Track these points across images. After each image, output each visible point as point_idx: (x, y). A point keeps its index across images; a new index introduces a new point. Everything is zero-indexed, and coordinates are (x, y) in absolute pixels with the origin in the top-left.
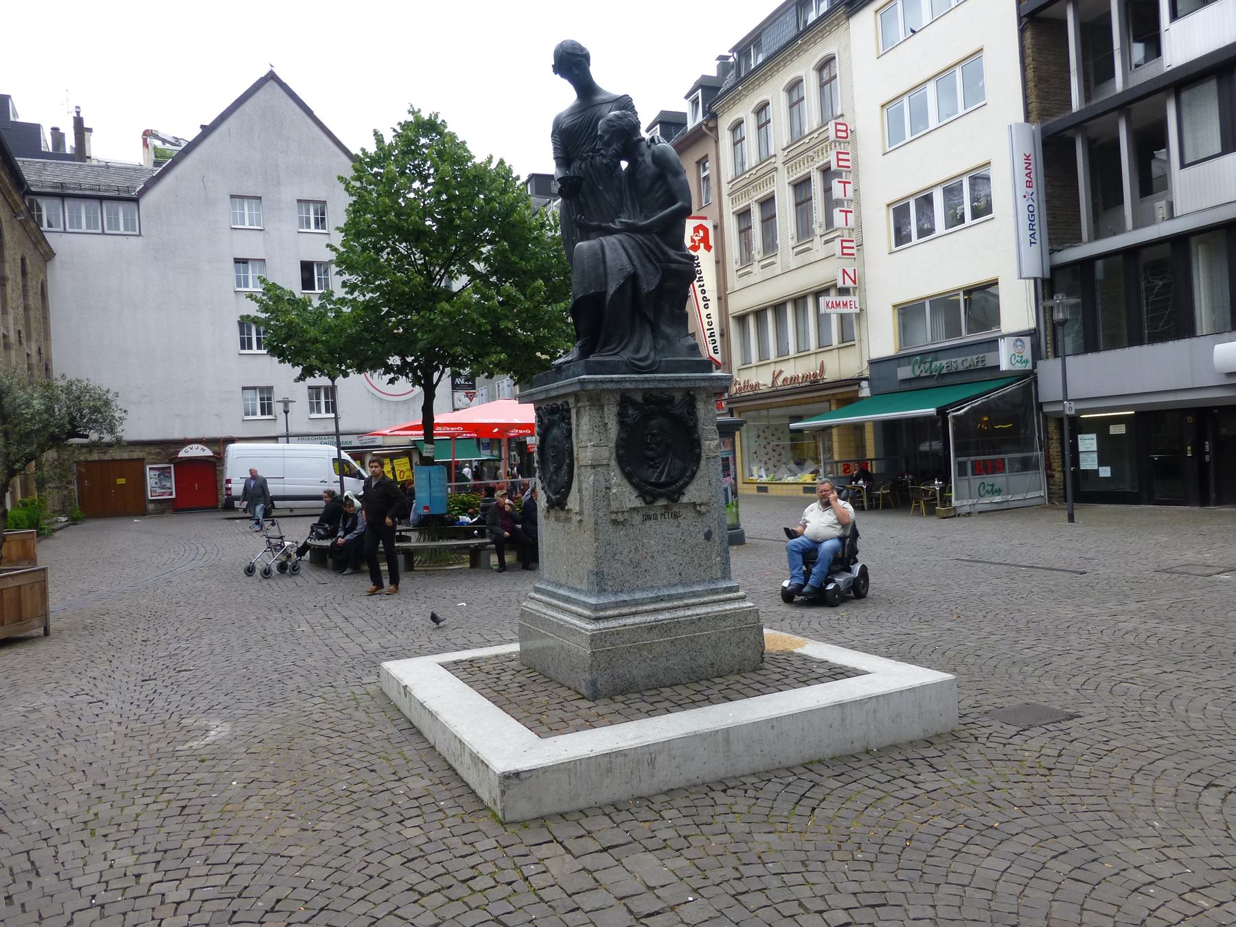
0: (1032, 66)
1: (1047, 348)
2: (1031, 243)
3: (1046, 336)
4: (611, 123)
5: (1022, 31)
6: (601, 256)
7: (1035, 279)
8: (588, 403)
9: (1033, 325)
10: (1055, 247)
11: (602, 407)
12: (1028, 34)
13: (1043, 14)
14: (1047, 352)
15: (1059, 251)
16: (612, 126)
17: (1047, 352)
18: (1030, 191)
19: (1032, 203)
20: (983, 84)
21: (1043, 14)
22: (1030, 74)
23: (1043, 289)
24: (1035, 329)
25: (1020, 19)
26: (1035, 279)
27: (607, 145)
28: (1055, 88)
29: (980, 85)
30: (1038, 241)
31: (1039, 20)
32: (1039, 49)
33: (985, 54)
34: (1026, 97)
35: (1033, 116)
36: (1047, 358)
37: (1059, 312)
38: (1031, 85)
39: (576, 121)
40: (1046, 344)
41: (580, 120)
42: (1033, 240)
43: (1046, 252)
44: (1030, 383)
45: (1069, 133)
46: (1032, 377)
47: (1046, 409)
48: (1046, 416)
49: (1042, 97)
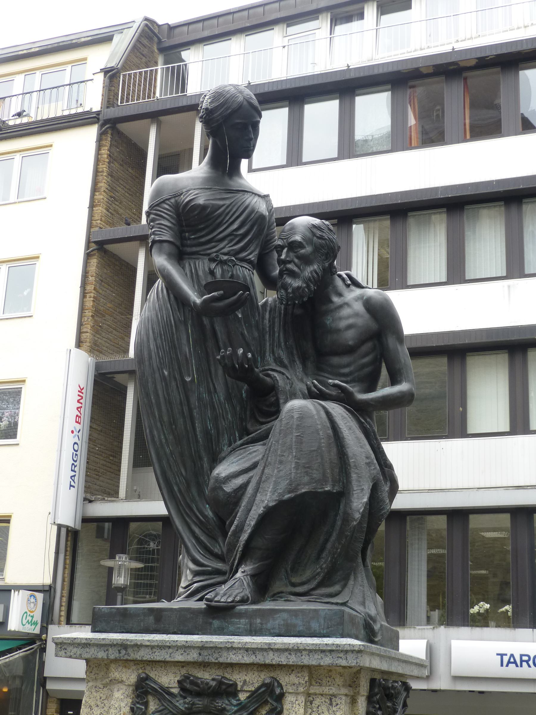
0: (92, 295)
1: (60, 611)
2: (71, 486)
3: (62, 596)
4: (319, 233)
5: (88, 256)
6: (330, 432)
7: (60, 527)
8: (344, 691)
9: (48, 580)
10: (89, 496)
11: (353, 701)
12: (94, 261)
13: (109, 247)
14: (60, 616)
15: (90, 501)
16: (321, 238)
17: (60, 616)
18: (78, 427)
19: (77, 441)
20: (30, 294)
21: (109, 247)
22: (89, 303)
23: (67, 540)
24: (50, 586)
25: (88, 242)
26: (60, 527)
27: (306, 260)
28: (108, 325)
29: (25, 293)
30: (76, 485)
31: (106, 252)
32: (101, 280)
33: (39, 264)
34: (80, 324)
35: (86, 345)
36: (59, 623)
37: (119, 575)
38: (88, 314)
39: (221, 203)
40: (61, 606)
41: (228, 202)
42: (72, 483)
43: (81, 499)
44: (35, 652)
45: (119, 378)
46: (38, 643)
47: (50, 686)
48: (47, 694)
49: (97, 330)
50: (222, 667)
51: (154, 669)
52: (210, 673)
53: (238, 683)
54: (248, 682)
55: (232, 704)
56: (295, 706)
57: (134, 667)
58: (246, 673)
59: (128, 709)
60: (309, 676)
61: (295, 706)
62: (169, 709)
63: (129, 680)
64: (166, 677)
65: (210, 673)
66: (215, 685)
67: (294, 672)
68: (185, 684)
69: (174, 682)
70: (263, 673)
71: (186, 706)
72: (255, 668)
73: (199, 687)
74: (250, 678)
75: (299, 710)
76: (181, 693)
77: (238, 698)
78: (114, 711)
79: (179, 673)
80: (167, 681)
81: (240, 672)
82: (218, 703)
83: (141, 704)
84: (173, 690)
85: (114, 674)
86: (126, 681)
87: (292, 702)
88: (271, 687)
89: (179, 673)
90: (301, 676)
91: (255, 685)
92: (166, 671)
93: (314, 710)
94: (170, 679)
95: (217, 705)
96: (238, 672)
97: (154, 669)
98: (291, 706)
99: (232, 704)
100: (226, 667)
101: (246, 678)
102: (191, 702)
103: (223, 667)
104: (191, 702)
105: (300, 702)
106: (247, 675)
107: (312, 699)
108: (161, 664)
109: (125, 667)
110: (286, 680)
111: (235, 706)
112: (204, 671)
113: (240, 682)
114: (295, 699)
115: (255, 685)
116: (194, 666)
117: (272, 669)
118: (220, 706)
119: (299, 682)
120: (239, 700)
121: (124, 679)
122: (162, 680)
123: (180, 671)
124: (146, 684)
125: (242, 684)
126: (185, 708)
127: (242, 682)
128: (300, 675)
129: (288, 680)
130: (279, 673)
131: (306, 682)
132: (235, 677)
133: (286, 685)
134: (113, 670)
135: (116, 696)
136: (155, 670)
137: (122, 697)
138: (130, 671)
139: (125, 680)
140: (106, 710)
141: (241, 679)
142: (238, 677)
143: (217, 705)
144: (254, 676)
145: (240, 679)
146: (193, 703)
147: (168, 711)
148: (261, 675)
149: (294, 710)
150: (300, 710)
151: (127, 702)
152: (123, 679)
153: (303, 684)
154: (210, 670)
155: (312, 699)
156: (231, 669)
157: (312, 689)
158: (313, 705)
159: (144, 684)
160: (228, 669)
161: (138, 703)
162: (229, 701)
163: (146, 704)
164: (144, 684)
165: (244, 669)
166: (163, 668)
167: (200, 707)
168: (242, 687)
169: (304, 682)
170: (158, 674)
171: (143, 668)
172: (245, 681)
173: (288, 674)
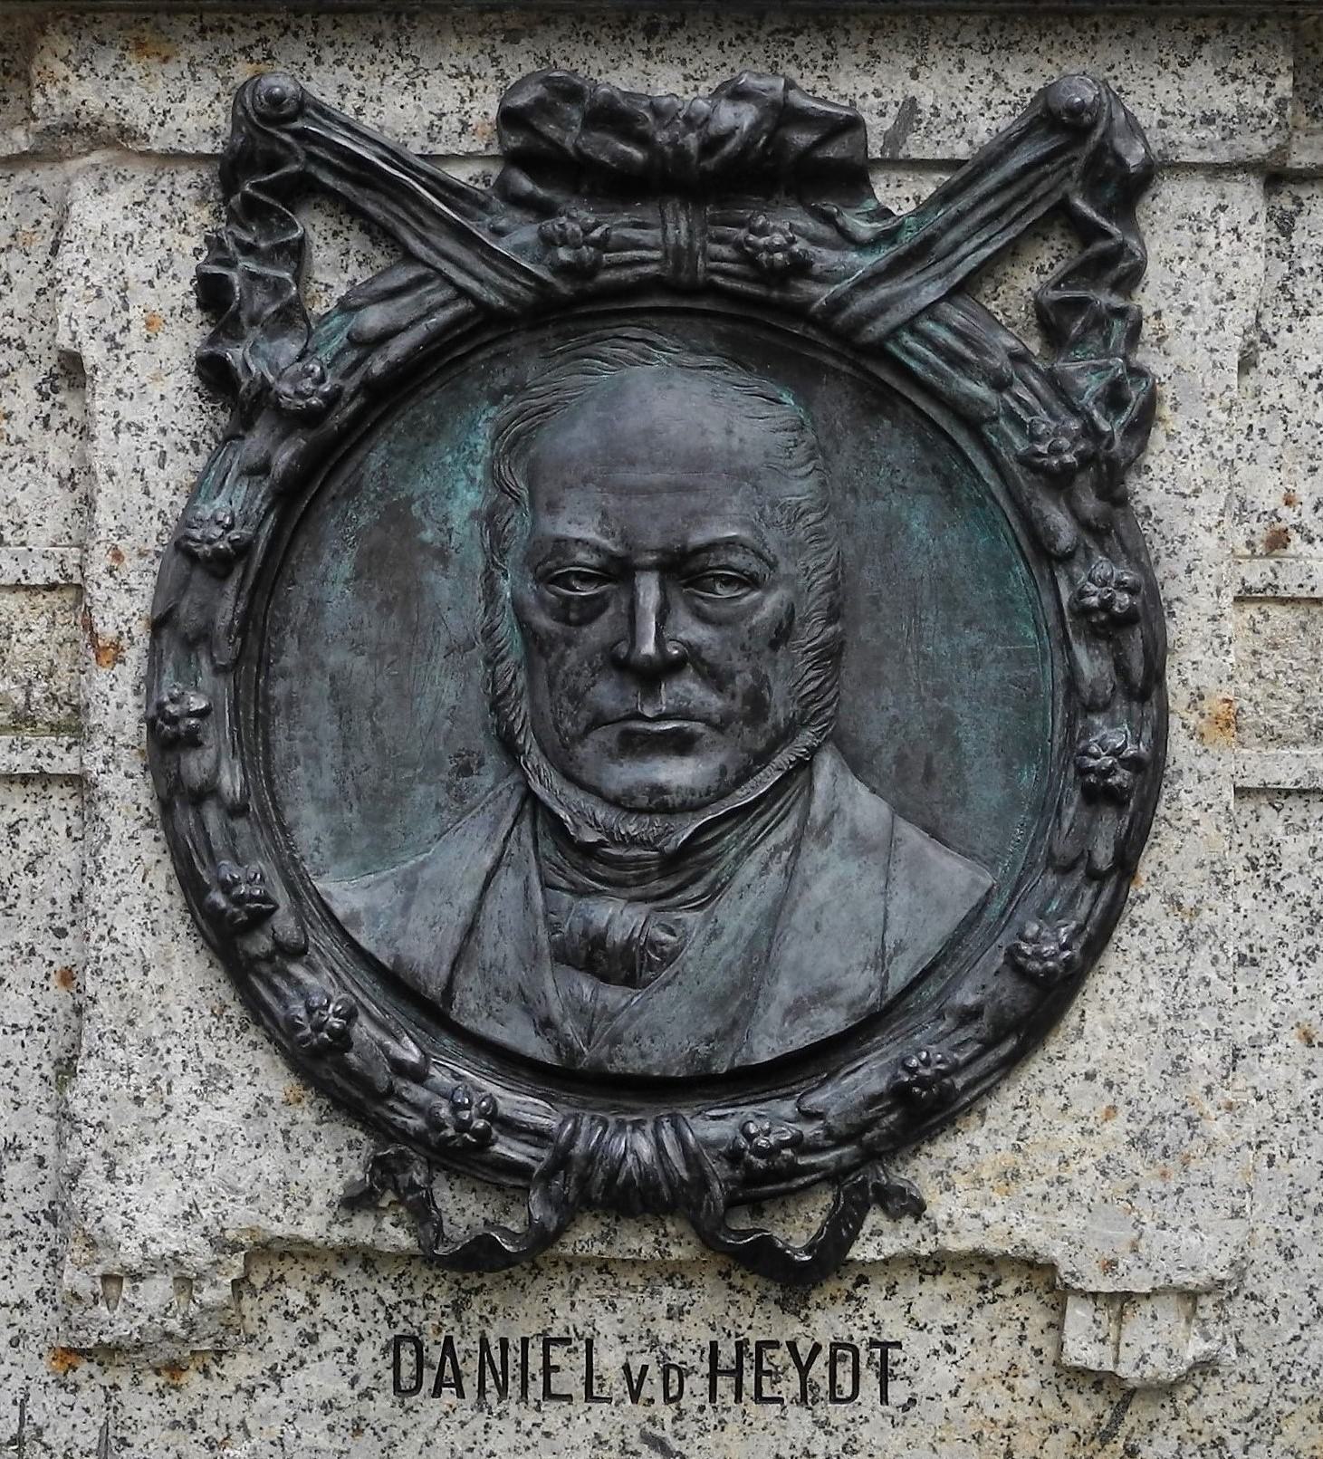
50: (763, 37)
51: (328, 55)
52: (690, 70)
53: (870, 119)
54: (928, 111)
55: (848, 240)
56: (1210, 239)
57: (198, 50)
58: (911, 64)
59: (180, 290)
60: (1295, 69)
61: (1210, 239)
62: (449, 281)
63: (170, 125)
64: (407, 98)
65: (690, 70)
66: (755, 126)
67: (1206, 50)
68: (551, 129)
69: (465, 125)
70: (1021, 61)
71: (564, 255)
72: (969, 35)
73: (643, 141)
74: (942, 89)
75: (1236, 264)
76: (525, 184)
77: (870, 205)
78: (82, 311)
79: (492, 72)
80: (421, 122)
81: (875, 56)
82: (762, 231)
83: (266, 258)
84: (460, 174)
85: (65, 92)
86: (153, 132)
87: (1196, 217)
88: (1099, 131)
89: (492, 72)
90: (1254, 69)
91: (969, 126)
92: (406, 66)
93: (1305, 264)
94: (436, 108)
95: (762, 241)
96: (862, 57)
97: (328, 55)
98: (1187, 243)
99: (848, 240)
100: (787, 30)
101: (915, 89)
102: (596, 234)
103: (768, 28)
104: (596, 234)
105: (1244, 219)
106: (921, 70)
107: (1289, 207)
108: (375, 27)
109: (140, 46)
110: (1161, 97)
111: (862, 246)
112: (648, 54)
113: (881, 114)
114: (1212, 201)
115: (969, 126)
116: (586, 27)
117: (1073, 35)
118: (779, 248)
119: (1240, 107)
120: (885, 213)
121: (139, 117)
122: (386, 119)
123: (496, 61)
124: (301, 135)
125: (888, 123)
126: (562, 270)
127: (893, 111)
128: (1244, 65)
129: (1175, 96)
130: (1116, 54)
131: (1281, 103)
132: (844, 87)
133: (1162, 125)
134: (61, 69)
135: (94, 222)
136: (339, 62)
137: (132, 225)
138: (172, 70)
139: (142, 124)
140: (22, 311)
141: (887, 97)
142: (866, 84)
143: (762, 241)
144: (963, 79)
145: (877, 94)
146: (605, 237)
147: (449, 292)
148: (1008, 74)
149: (1208, 261)
150: (1244, 261)
151: (162, 253)
152: (128, 120)
153: (1263, 116)
154: (688, 52)
155: (1289, 207)
156: (822, 41)
157: (1304, 148)
158: (1298, 238)
159: (287, 138)
160: (800, 42)
161: (248, 250)
162: (828, 219)
163: (297, 253)
164: (287, 138)
165: (902, 42)
166: (391, 45)
167: (643, 262)
168: (892, 139)
169: (1270, 102)
170: (360, 83)
171: (258, 53)
172: (910, 108)
173: (1174, 66)
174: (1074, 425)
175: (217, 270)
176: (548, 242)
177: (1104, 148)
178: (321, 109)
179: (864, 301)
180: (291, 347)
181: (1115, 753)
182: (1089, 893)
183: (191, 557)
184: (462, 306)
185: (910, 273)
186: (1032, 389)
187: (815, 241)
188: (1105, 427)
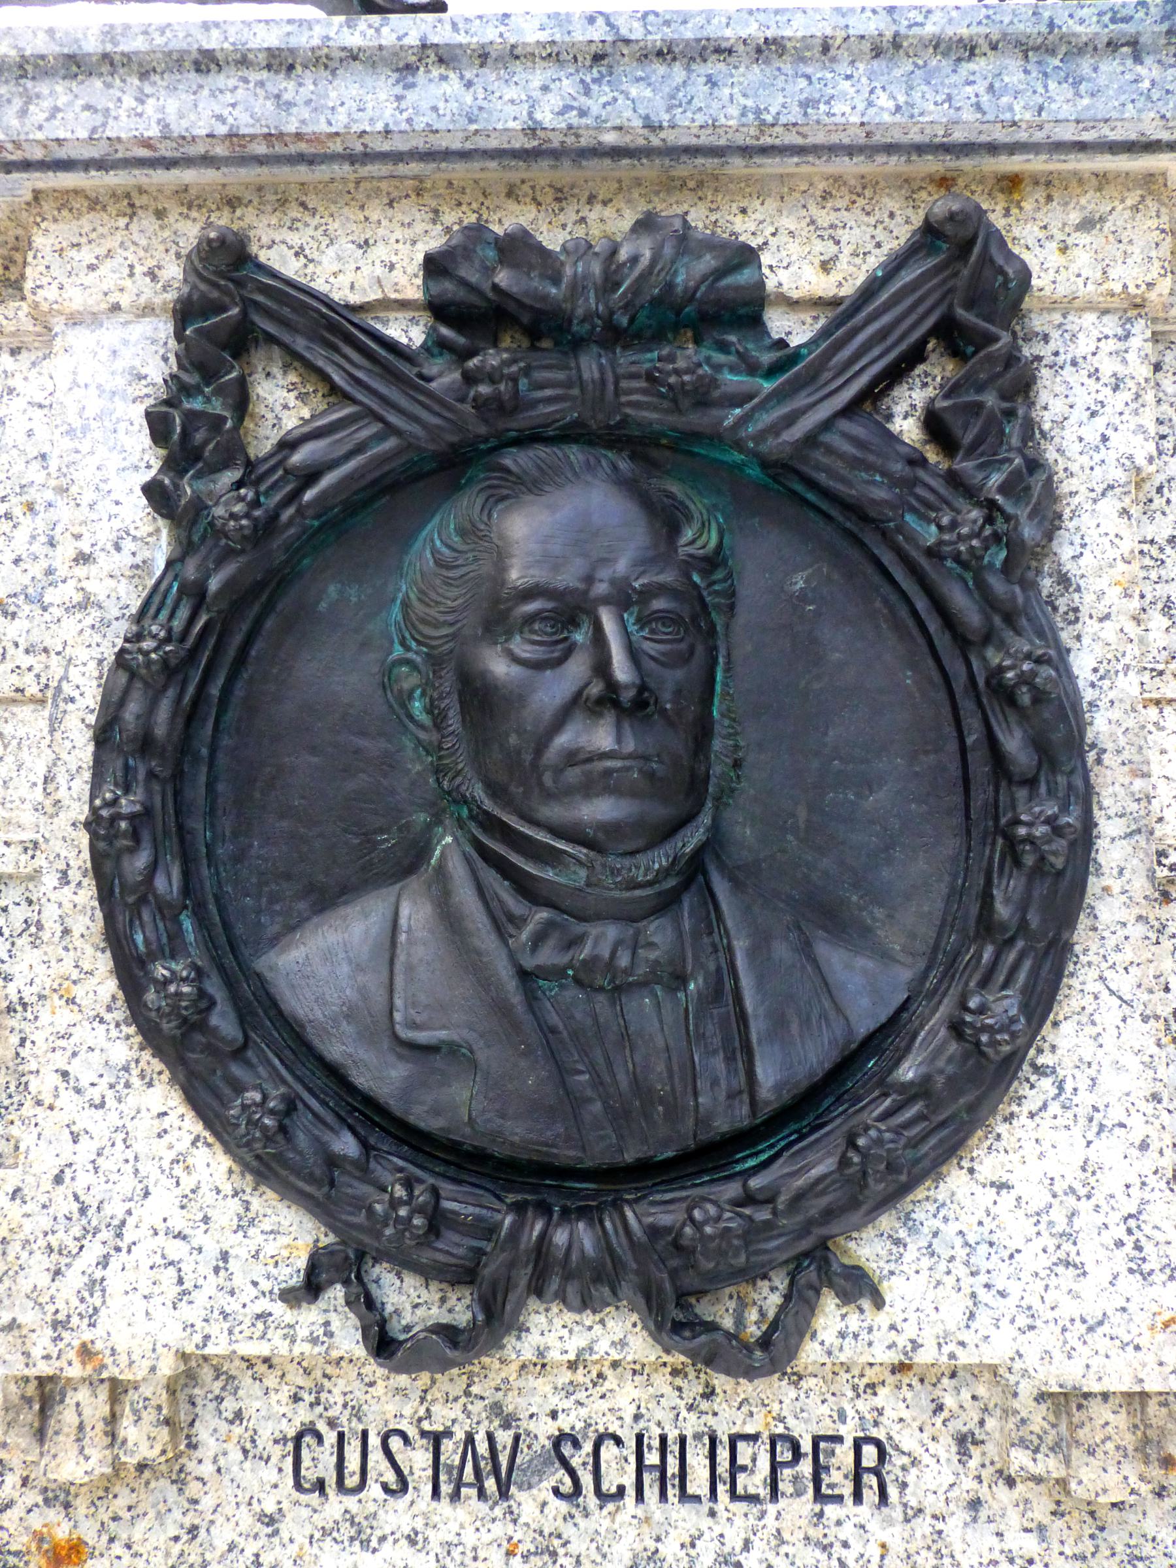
120: (782, 344)
163: (242, 401)
174: (975, 514)
175: (164, 409)
176: (470, 379)
177: (986, 259)
178: (261, 267)
179: (766, 419)
180: (230, 476)
181: (1049, 821)
182: (1027, 965)
183: (133, 676)
184: (391, 443)
185: (810, 389)
186: (932, 490)
187: (718, 368)
188: (1010, 509)
